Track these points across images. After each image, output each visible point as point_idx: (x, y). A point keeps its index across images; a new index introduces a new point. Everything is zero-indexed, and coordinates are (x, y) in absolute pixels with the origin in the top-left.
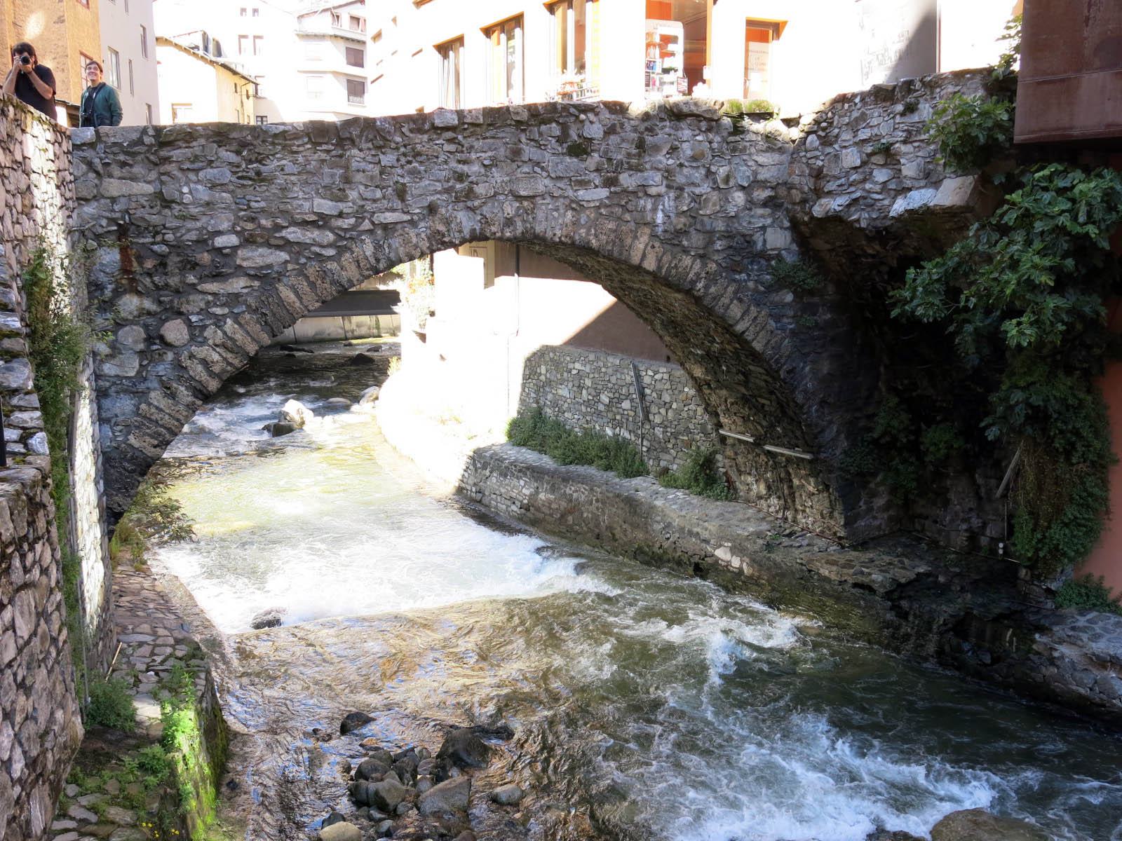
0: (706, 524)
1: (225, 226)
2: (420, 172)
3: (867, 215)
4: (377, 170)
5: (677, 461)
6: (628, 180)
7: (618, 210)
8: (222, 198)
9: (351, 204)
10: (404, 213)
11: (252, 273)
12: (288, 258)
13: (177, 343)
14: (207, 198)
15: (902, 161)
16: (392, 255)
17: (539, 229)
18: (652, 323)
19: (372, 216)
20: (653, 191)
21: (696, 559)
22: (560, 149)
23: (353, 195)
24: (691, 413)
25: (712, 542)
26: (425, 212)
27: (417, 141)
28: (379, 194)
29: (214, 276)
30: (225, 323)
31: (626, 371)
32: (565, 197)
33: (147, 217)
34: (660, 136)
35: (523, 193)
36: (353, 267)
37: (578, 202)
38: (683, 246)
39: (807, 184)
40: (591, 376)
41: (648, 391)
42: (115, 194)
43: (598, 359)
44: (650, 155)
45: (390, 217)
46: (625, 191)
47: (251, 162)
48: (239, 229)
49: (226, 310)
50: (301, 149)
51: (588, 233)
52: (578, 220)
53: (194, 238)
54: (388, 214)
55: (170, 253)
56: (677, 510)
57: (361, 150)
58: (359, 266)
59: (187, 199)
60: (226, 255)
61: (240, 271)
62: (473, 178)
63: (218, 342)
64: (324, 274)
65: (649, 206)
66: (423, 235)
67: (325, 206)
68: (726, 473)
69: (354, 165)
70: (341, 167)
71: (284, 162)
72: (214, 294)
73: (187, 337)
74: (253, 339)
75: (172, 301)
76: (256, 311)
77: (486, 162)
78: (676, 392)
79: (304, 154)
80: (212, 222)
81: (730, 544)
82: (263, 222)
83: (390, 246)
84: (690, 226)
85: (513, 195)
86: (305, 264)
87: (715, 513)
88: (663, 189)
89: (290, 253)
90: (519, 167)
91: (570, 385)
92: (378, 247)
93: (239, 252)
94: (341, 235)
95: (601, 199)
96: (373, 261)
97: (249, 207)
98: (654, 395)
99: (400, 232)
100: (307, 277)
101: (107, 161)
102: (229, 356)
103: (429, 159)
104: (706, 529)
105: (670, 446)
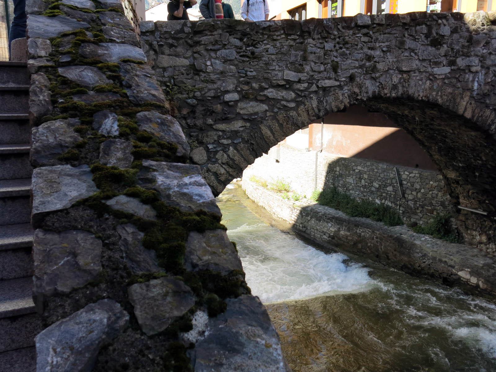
0: (452, 257)
1: (231, 87)
2: (346, 55)
4: (322, 53)
5: (423, 219)
6: (461, 62)
7: (454, 81)
8: (230, 69)
9: (306, 74)
10: (336, 80)
11: (246, 117)
12: (267, 109)
13: (200, 162)
14: (221, 69)
16: (328, 107)
17: (411, 92)
18: (428, 149)
19: (317, 82)
20: (474, 69)
21: (445, 275)
22: (426, 41)
23: (307, 68)
24: (434, 195)
25: (456, 267)
26: (348, 80)
27: (346, 34)
28: (322, 68)
29: (223, 120)
30: (229, 149)
31: (390, 172)
32: (426, 72)
33: (185, 80)
34: (480, 35)
35: (404, 69)
36: (305, 114)
37: (433, 75)
38: (487, 104)
40: (368, 173)
41: (405, 182)
42: (166, 65)
43: (372, 165)
44: (474, 47)
45: (328, 83)
46: (459, 69)
47: (248, 46)
48: (239, 89)
49: (230, 141)
50: (279, 38)
51: (437, 95)
52: (433, 86)
53: (212, 95)
54: (326, 81)
55: (198, 104)
56: (428, 246)
57: (314, 39)
58: (308, 114)
59: (210, 69)
60: (230, 106)
61: (239, 116)
62: (376, 59)
63: (224, 161)
65: (471, 79)
66: (346, 95)
67: (291, 75)
68: (457, 228)
69: (309, 49)
70: (302, 50)
71: (268, 46)
72: (223, 131)
73: (206, 158)
74: (245, 159)
75: (198, 136)
76: (247, 142)
77: (384, 49)
78: (425, 184)
79: (280, 41)
80: (224, 85)
81: (469, 270)
82: (254, 85)
83: (327, 102)
84: (491, 91)
85: (398, 70)
86: (277, 112)
87: (454, 250)
88: (479, 68)
89: (268, 105)
90: (403, 52)
91: (354, 177)
92: (320, 102)
93: (239, 104)
95: (446, 74)
96: (316, 110)
97: (246, 75)
98: (409, 184)
99: (333, 92)
100: (278, 121)
101: (161, 43)
102: (230, 170)
103: (352, 46)
104: (452, 260)
105: (418, 211)
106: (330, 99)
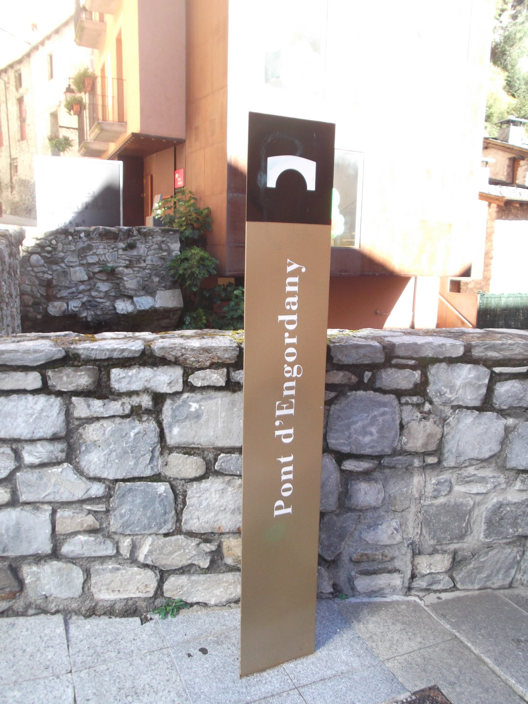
3: (93, 313)
15: (125, 278)
39: (38, 291)
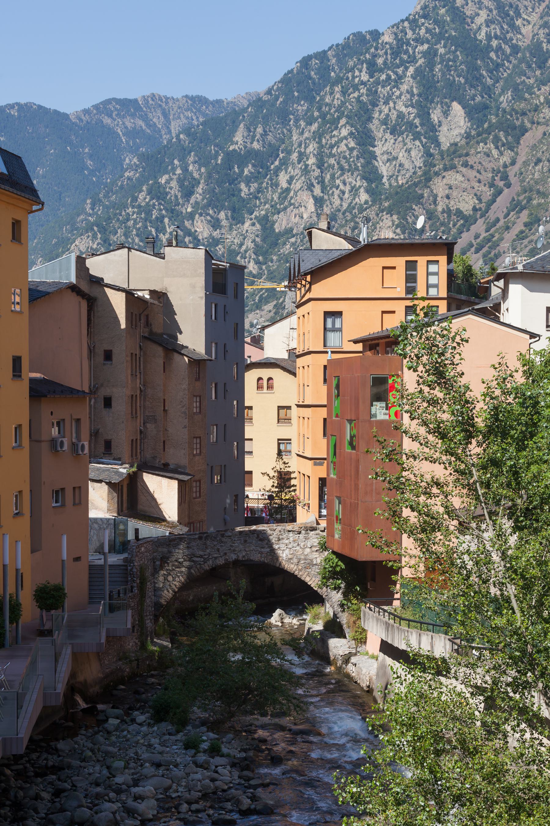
17: (251, 558)
45: (216, 555)
64: (201, 567)
67: (201, 553)
92: (213, 562)
94: (205, 559)
106: (217, 561)
